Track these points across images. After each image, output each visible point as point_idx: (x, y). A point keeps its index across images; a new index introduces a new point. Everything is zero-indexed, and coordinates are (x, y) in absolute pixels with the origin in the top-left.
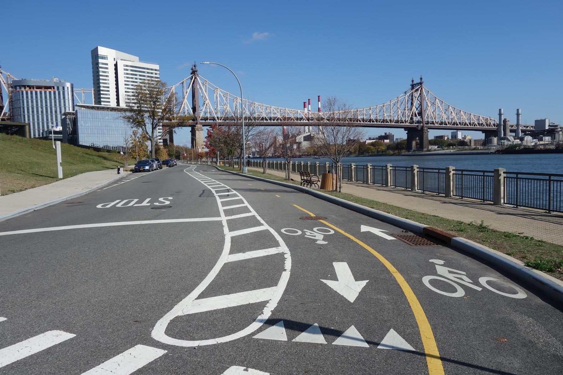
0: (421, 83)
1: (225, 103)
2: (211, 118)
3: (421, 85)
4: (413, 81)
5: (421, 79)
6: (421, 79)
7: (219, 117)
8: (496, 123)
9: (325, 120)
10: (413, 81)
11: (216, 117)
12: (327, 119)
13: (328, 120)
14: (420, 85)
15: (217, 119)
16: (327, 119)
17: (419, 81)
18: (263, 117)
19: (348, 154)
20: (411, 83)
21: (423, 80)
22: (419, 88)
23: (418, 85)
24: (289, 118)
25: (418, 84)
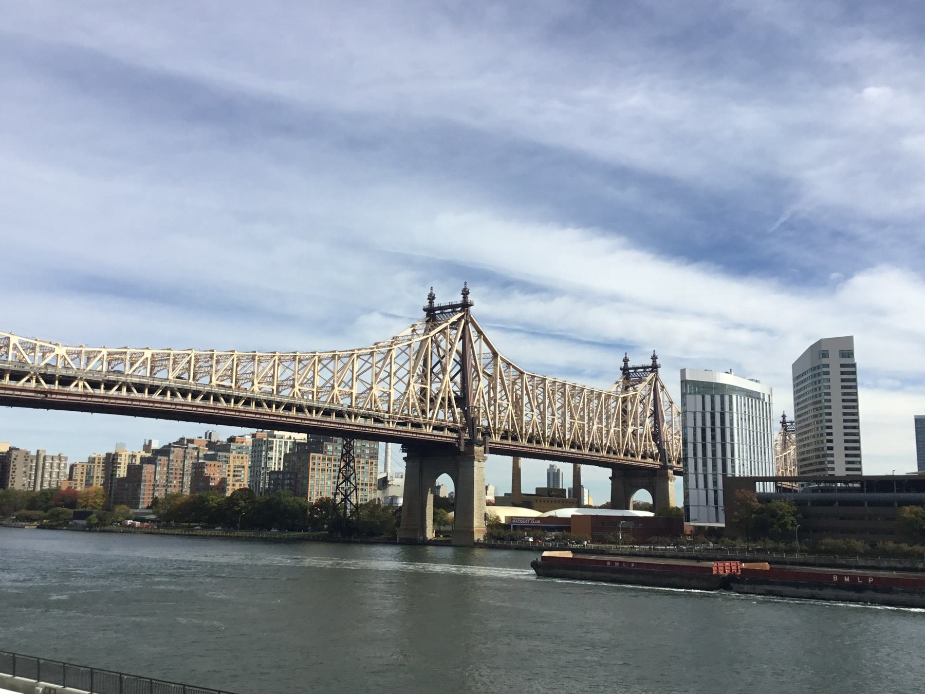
0: (465, 305)
3: (467, 310)
14: (460, 312)
17: (459, 299)
19: (132, 528)
22: (459, 319)
23: (454, 312)
25: (453, 307)
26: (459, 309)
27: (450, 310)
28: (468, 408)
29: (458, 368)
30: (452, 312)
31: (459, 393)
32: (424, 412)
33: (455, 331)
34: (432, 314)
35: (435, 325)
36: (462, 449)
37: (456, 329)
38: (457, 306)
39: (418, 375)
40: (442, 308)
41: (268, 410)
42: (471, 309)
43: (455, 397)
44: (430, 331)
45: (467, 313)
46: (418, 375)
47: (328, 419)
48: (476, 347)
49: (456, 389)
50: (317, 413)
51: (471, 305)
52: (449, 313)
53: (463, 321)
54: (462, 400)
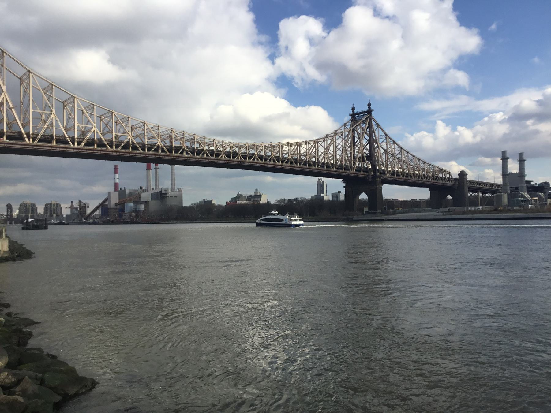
0: (370, 111)
1: (46, 104)
2: (11, 134)
4: (353, 109)
5: (369, 105)
6: (369, 105)
7: (31, 132)
8: (451, 177)
9: (239, 158)
10: (353, 109)
11: (23, 131)
12: (241, 156)
13: (245, 157)
15: (25, 136)
16: (241, 156)
17: (366, 109)
18: (128, 142)
20: (351, 112)
21: (372, 107)
22: (367, 119)
24: (177, 149)
25: (364, 113)
26: (366, 113)
27: (362, 114)
28: (373, 161)
29: (368, 142)
30: (363, 115)
31: (368, 154)
32: (350, 163)
33: (364, 125)
34: (354, 116)
35: (355, 123)
36: (370, 180)
37: (365, 123)
38: (365, 112)
39: (348, 146)
40: (357, 114)
41: (314, 167)
42: (372, 112)
43: (366, 156)
44: (353, 126)
45: (371, 115)
46: (348, 146)
47: (323, 169)
48: (376, 132)
49: (367, 152)
50: (318, 166)
51: (373, 111)
52: (362, 116)
53: (369, 119)
54: (370, 157)
